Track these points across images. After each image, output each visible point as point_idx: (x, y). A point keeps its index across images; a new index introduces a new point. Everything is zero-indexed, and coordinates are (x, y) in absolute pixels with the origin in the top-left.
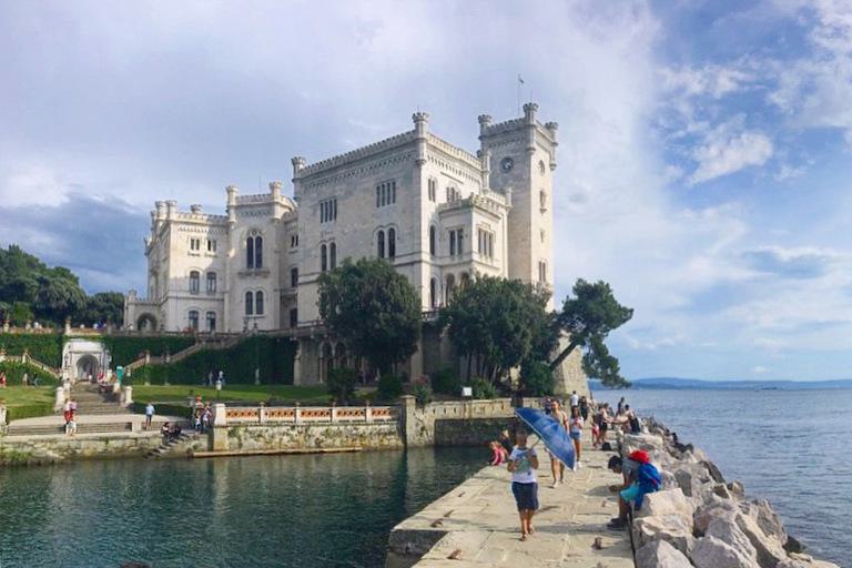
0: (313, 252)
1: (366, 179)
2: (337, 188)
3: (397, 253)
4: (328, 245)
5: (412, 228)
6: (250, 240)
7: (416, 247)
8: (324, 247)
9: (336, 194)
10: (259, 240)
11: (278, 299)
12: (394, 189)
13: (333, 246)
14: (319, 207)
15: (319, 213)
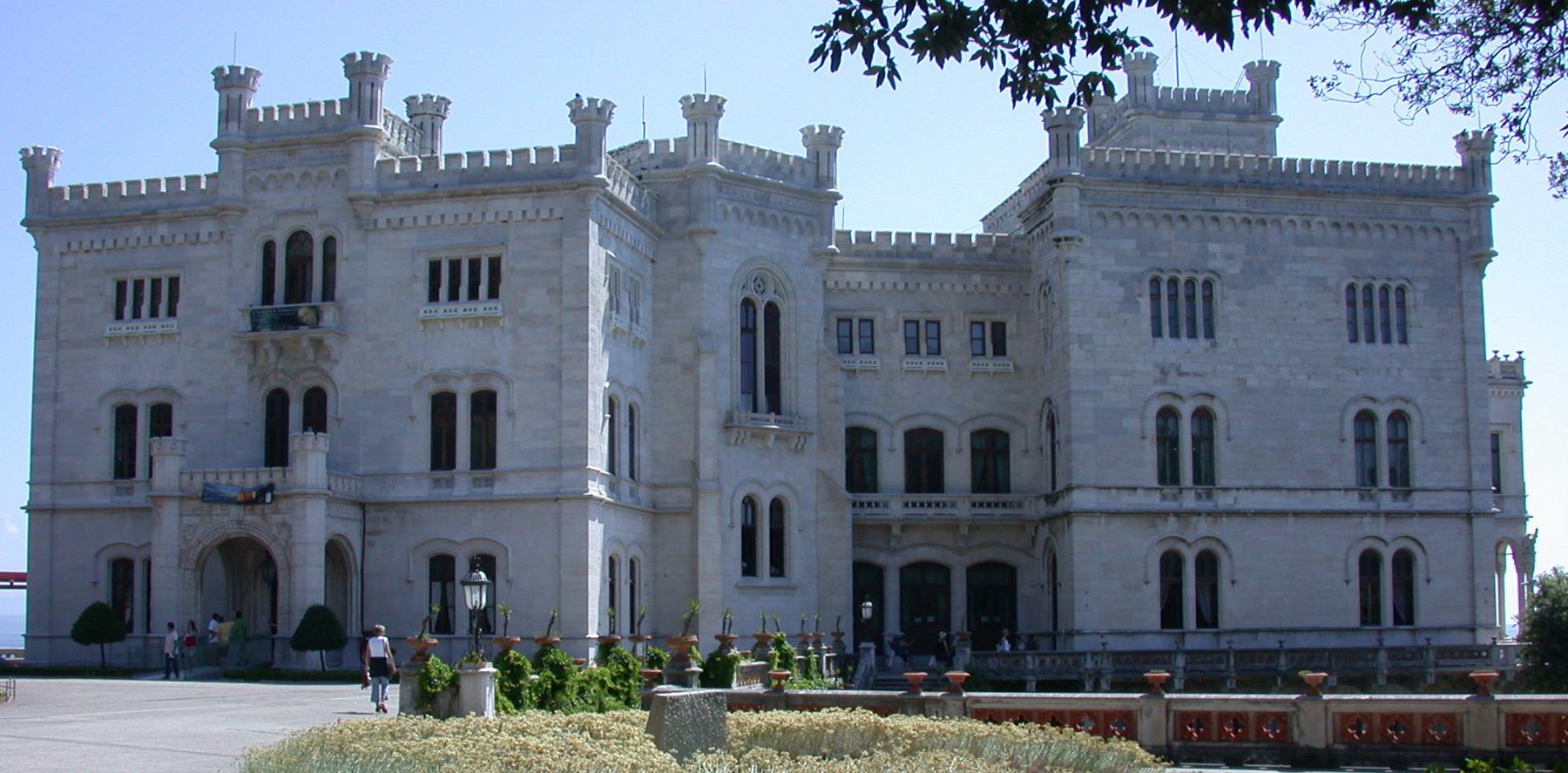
0: (1130, 423)
1: (1310, 251)
2: (1214, 247)
3: (1418, 478)
4: (1186, 410)
5: (1467, 420)
6: (747, 304)
7: (1476, 476)
8: (1168, 415)
9: (1212, 264)
10: (772, 312)
11: (849, 531)
12: (1401, 304)
13: (1204, 416)
14: (1147, 287)
15: (1145, 303)
